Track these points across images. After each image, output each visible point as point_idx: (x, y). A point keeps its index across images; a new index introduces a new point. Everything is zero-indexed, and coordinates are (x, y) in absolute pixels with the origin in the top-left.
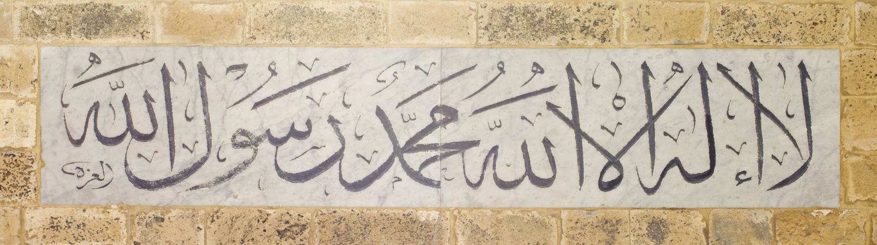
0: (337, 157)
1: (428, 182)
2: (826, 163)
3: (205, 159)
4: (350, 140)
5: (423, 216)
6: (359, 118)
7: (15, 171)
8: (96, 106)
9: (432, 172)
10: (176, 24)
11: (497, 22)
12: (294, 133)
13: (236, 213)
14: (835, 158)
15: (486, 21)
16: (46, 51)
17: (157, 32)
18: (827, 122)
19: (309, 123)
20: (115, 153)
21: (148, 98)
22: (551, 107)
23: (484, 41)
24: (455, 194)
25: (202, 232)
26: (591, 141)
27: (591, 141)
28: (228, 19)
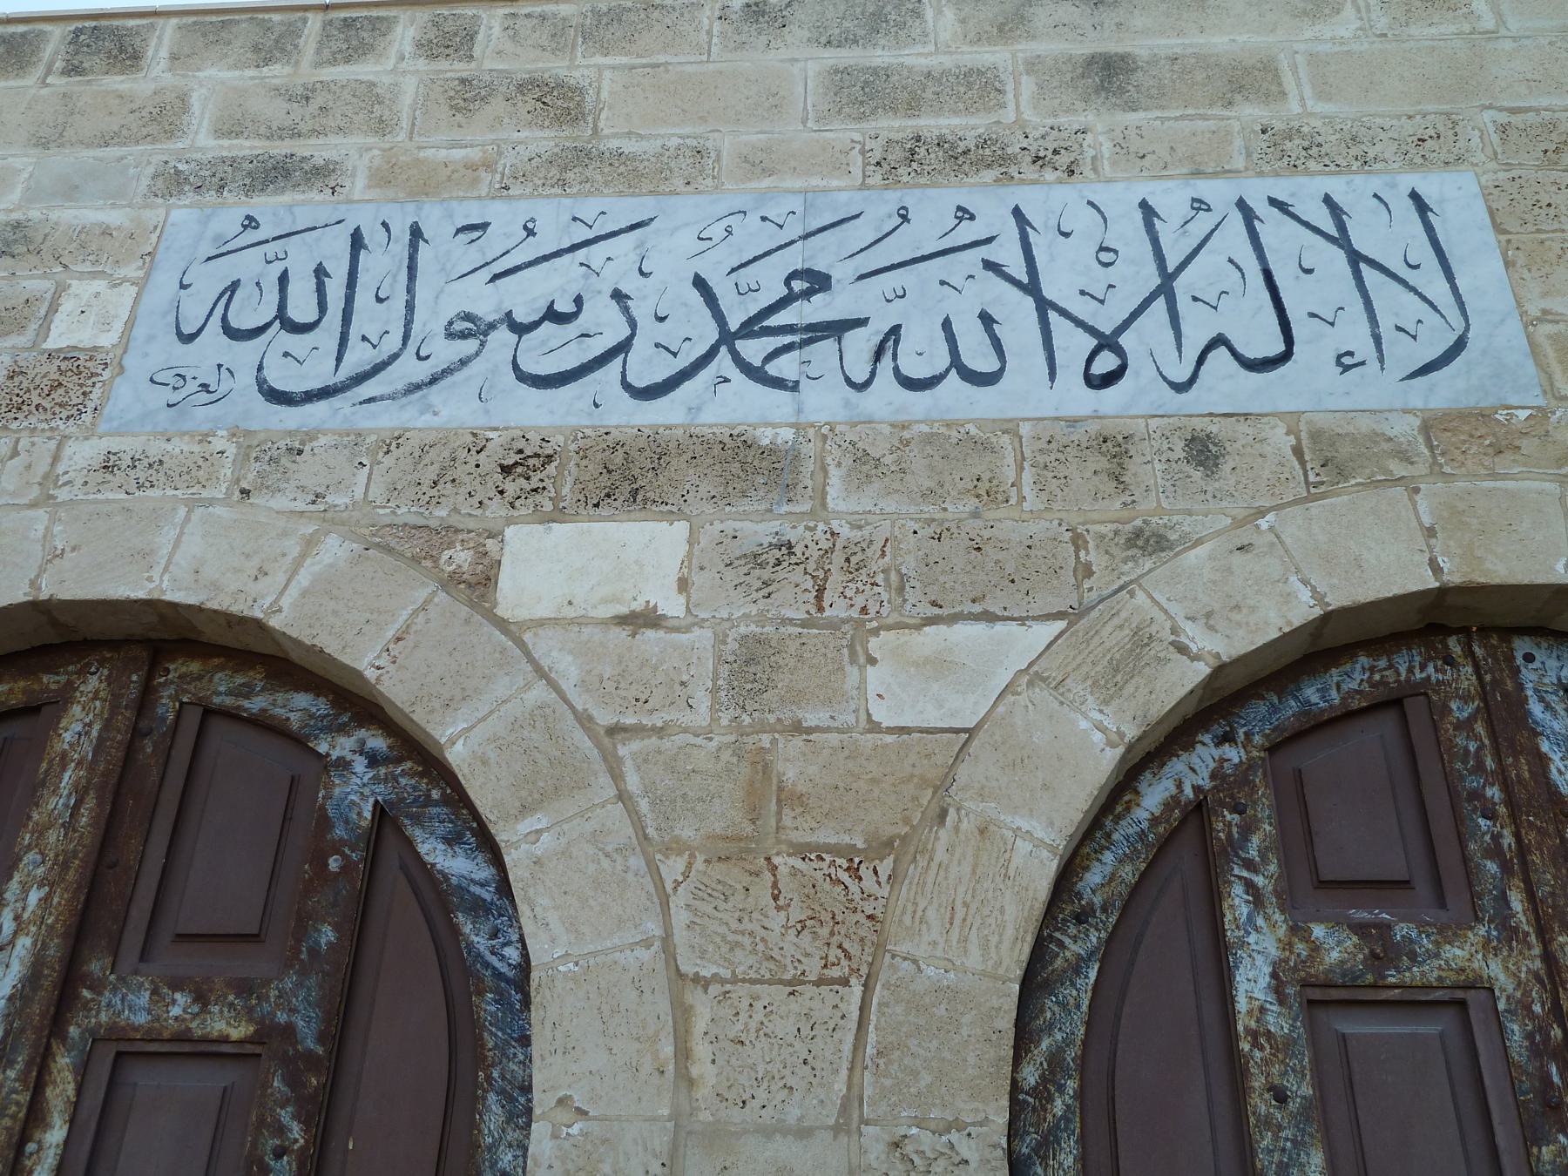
0: (623, 347)
1: (778, 383)
3: (394, 357)
5: (765, 437)
7: (70, 381)
8: (234, 286)
9: (784, 367)
11: (896, 155)
14: (1514, 327)
15: (877, 155)
16: (176, 215)
17: (358, 186)
18: (1482, 272)
19: (578, 301)
20: (247, 352)
21: (320, 273)
22: (989, 265)
23: (876, 179)
24: (824, 401)
25: (366, 470)
26: (1064, 313)
27: (1064, 313)
28: (472, 167)
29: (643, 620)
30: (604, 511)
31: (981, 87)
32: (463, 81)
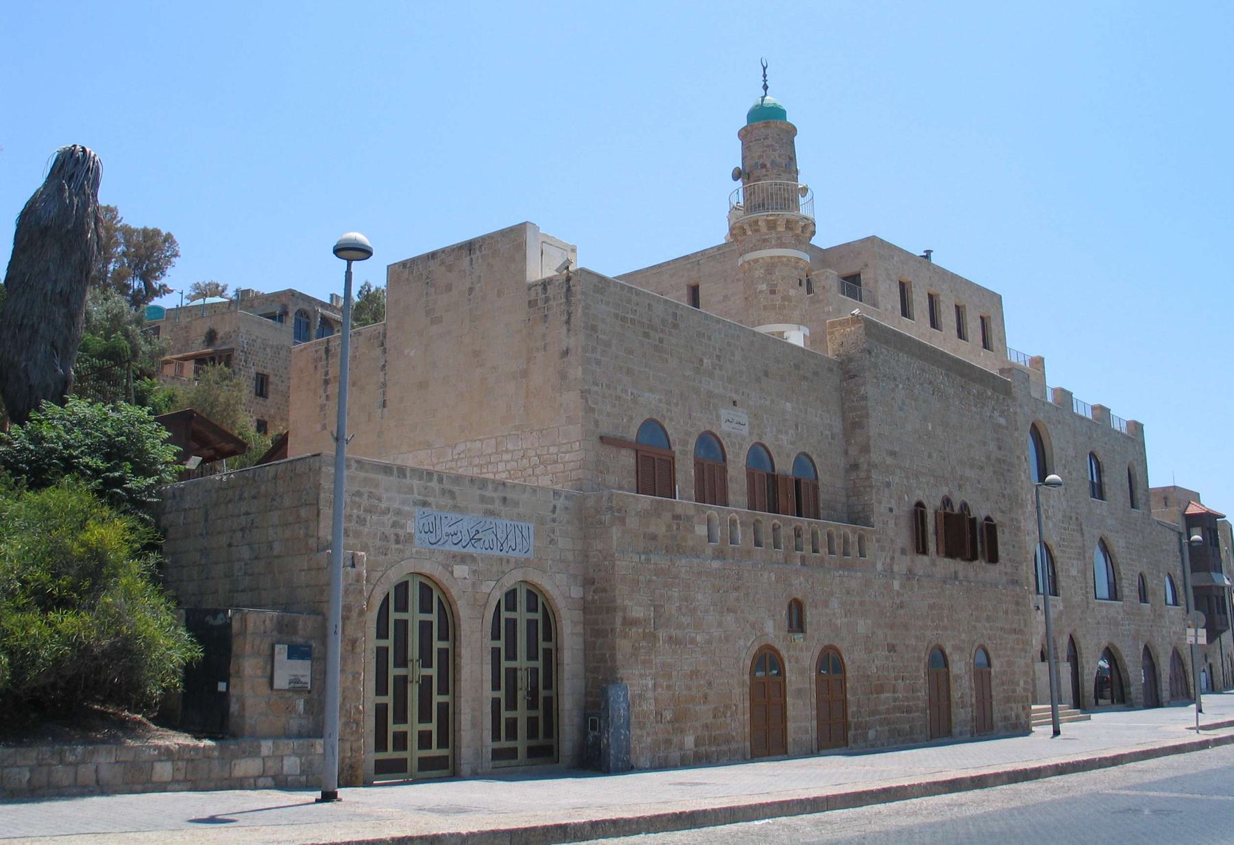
2: (531, 548)
6: (465, 532)
31: (492, 500)
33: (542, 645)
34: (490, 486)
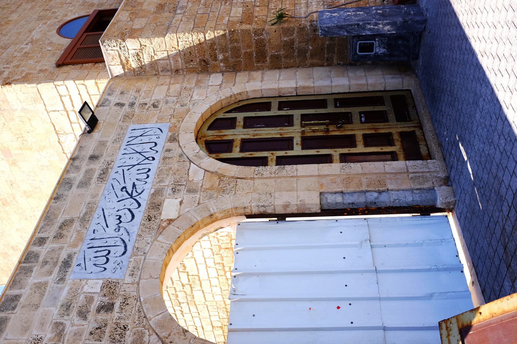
1: (142, 192)
2: (159, 125)
4: (125, 207)
9: (139, 191)
10: (75, 246)
12: (119, 219)
13: (140, 230)
18: (147, 126)
21: (96, 252)
22: (128, 170)
23: (105, 182)
29: (181, 203)
30: (161, 208)
32: (54, 238)
33: (274, 112)
34: (71, 175)
